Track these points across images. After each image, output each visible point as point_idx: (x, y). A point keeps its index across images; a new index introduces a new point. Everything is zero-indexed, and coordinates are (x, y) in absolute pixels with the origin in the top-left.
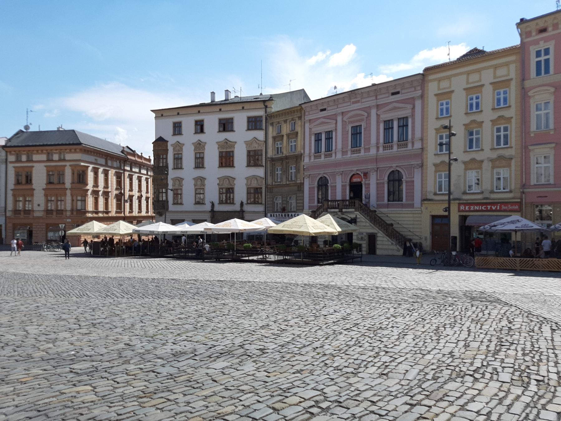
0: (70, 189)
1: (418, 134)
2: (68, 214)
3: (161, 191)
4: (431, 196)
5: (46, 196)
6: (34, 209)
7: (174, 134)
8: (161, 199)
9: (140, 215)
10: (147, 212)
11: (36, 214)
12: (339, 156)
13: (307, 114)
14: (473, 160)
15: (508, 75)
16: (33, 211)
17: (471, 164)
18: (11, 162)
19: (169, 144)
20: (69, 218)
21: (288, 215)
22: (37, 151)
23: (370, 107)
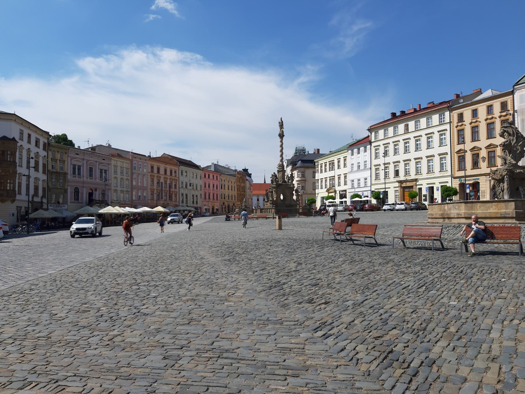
1: (110, 178)
4: (113, 201)
12: (85, 179)
13: (69, 152)
14: (122, 190)
15: (128, 166)
17: (122, 191)
19: (19, 144)
21: (60, 206)
23: (96, 161)
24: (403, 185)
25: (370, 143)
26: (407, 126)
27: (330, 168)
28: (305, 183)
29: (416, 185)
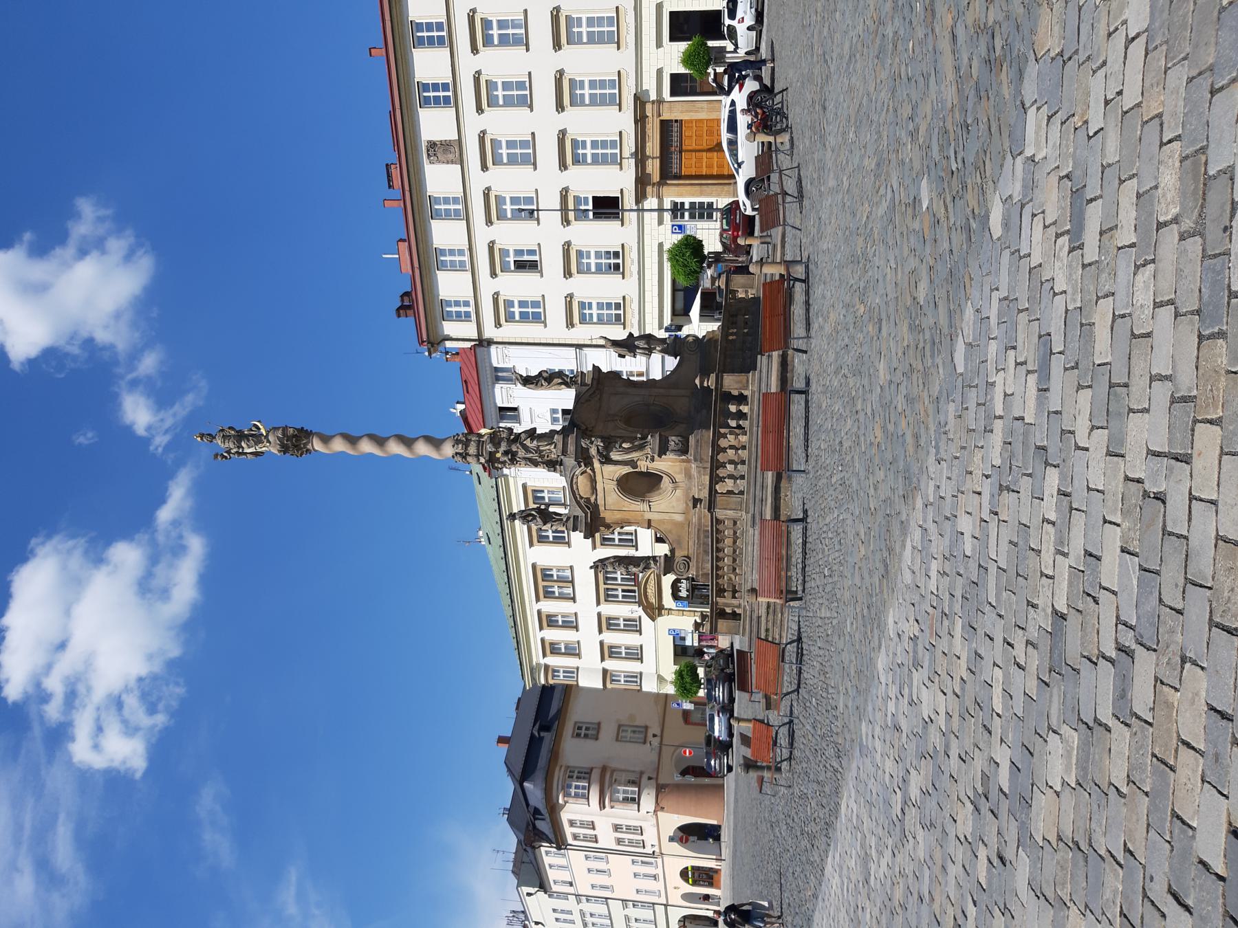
24: (656, 177)
25: (483, 343)
26: (439, 150)
27: (563, 597)
28: (613, 771)
29: (660, 101)
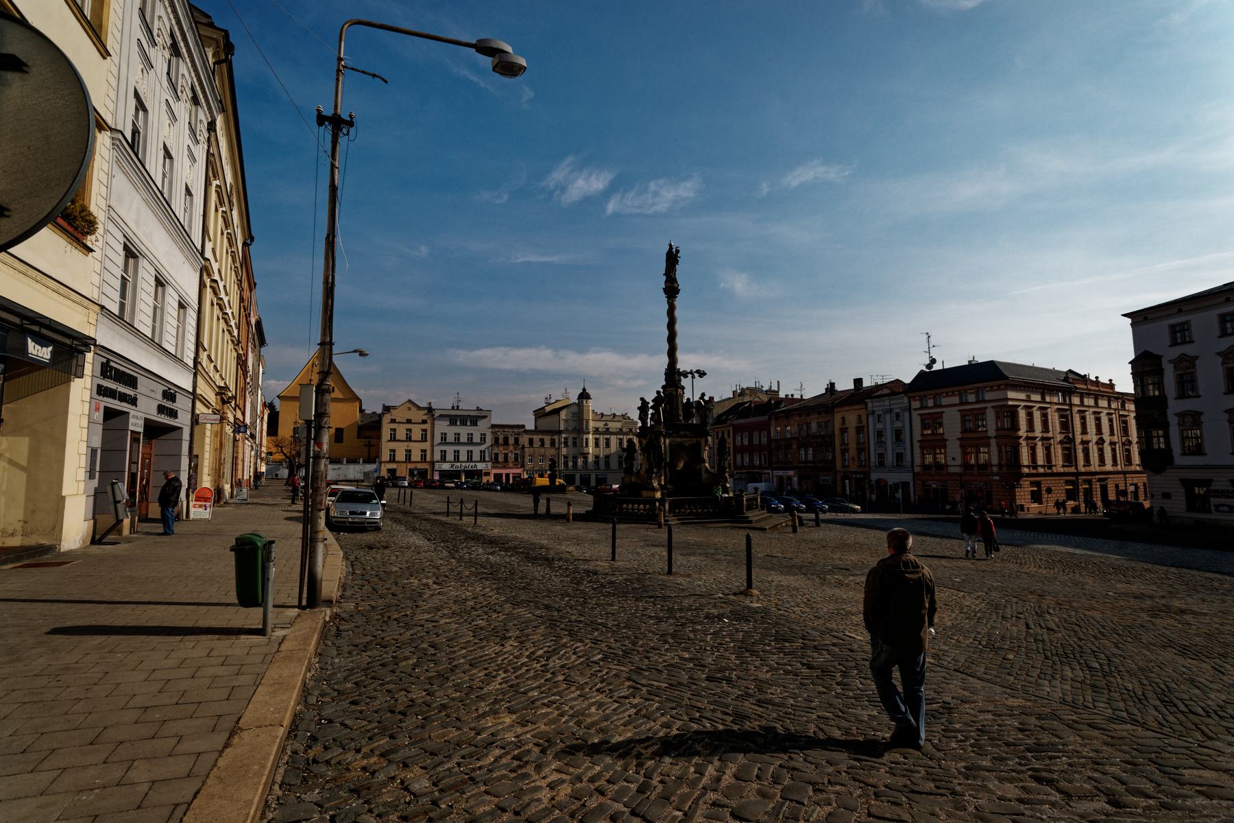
0: (995, 437)
2: (995, 469)
3: (1155, 433)
5: (963, 447)
6: (948, 464)
7: (1174, 343)
8: (1156, 447)
9: (1103, 469)
10: (1115, 463)
11: (951, 470)
16: (947, 466)
18: (915, 409)
19: (1164, 361)
20: (996, 474)
22: (947, 393)
